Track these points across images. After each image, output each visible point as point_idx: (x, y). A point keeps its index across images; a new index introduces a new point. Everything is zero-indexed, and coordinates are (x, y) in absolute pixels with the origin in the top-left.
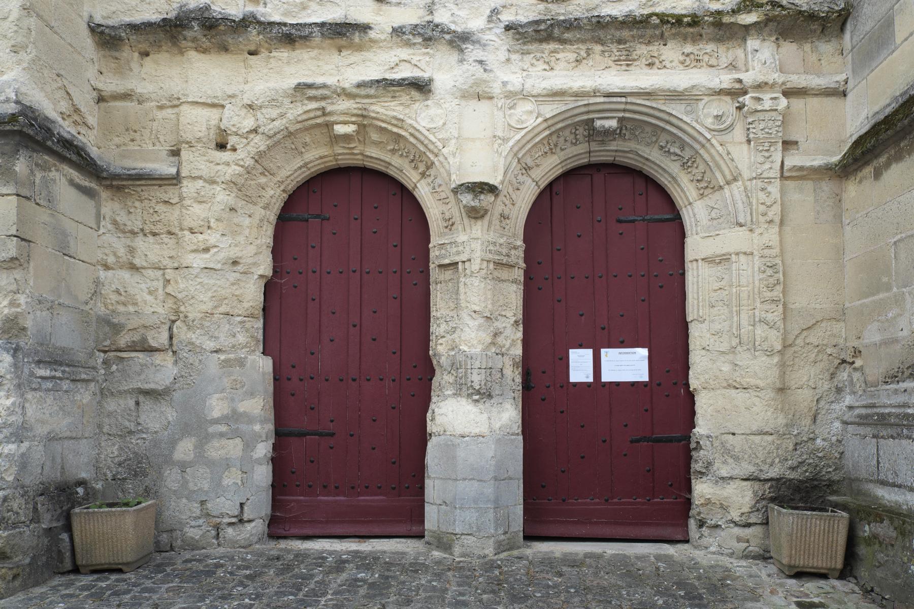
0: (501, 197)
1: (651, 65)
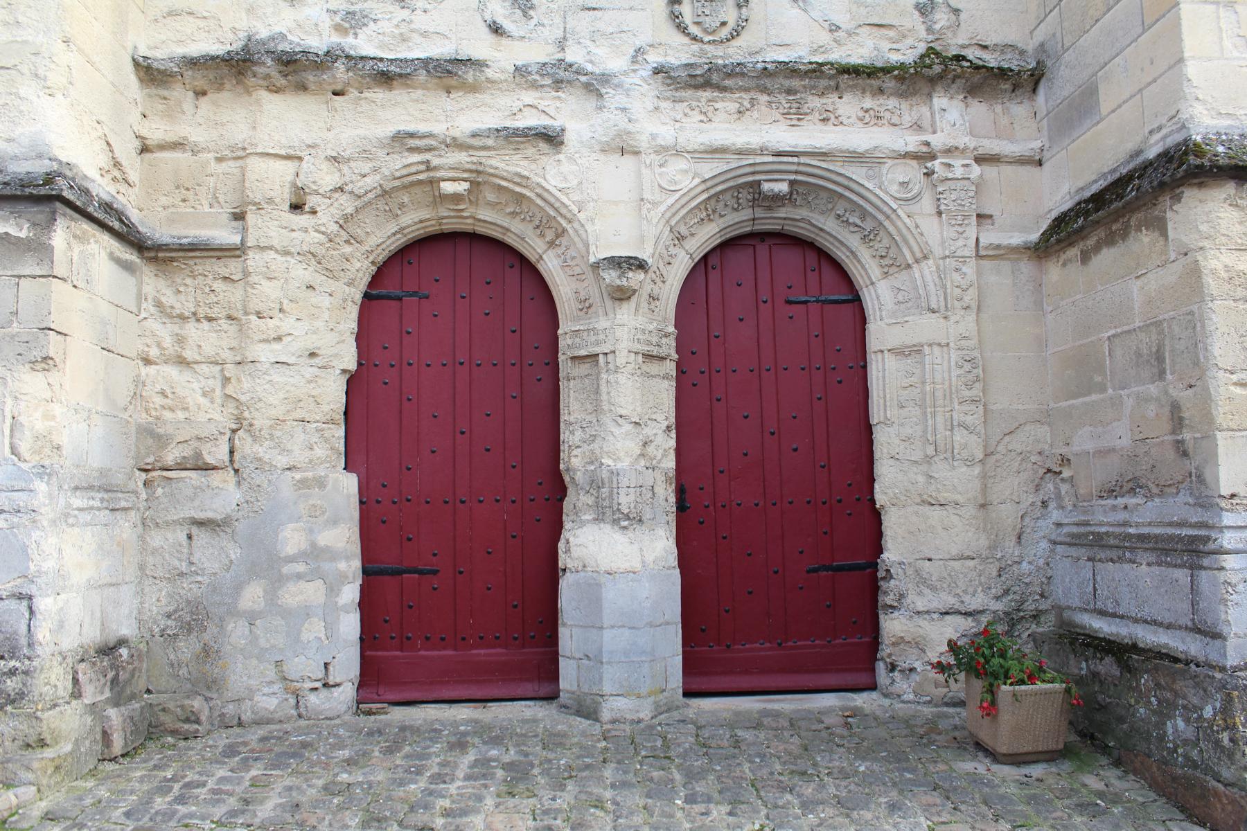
0: (651, 274)
1: (825, 120)
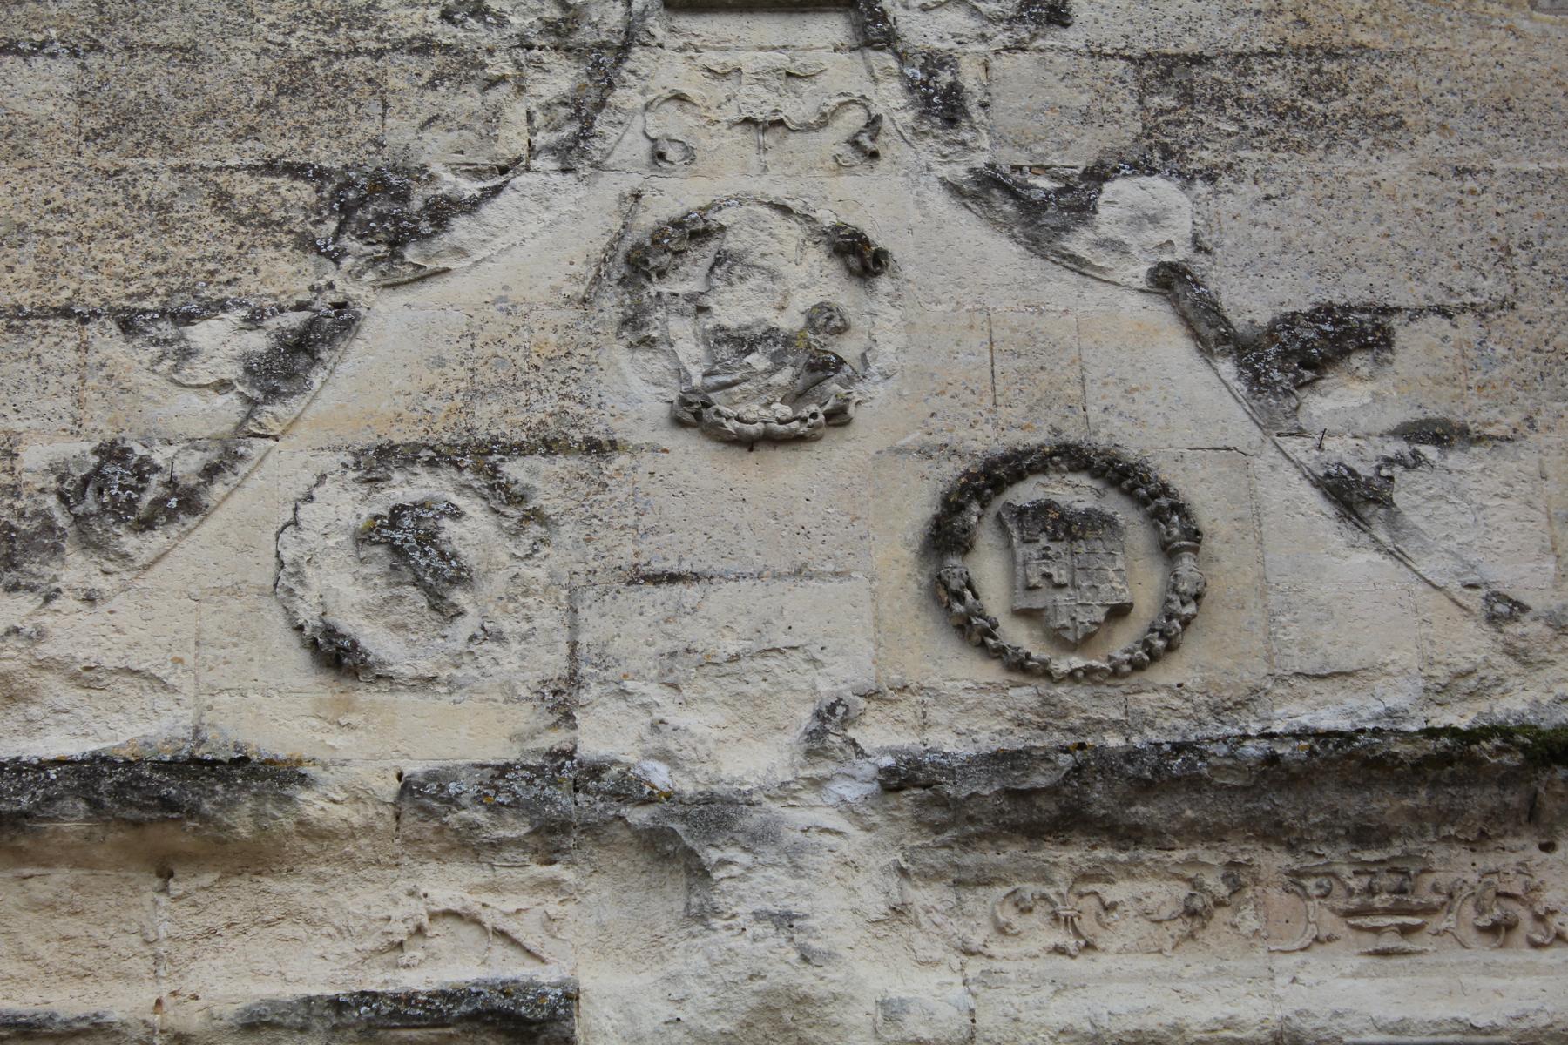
1: (1499, 930)
